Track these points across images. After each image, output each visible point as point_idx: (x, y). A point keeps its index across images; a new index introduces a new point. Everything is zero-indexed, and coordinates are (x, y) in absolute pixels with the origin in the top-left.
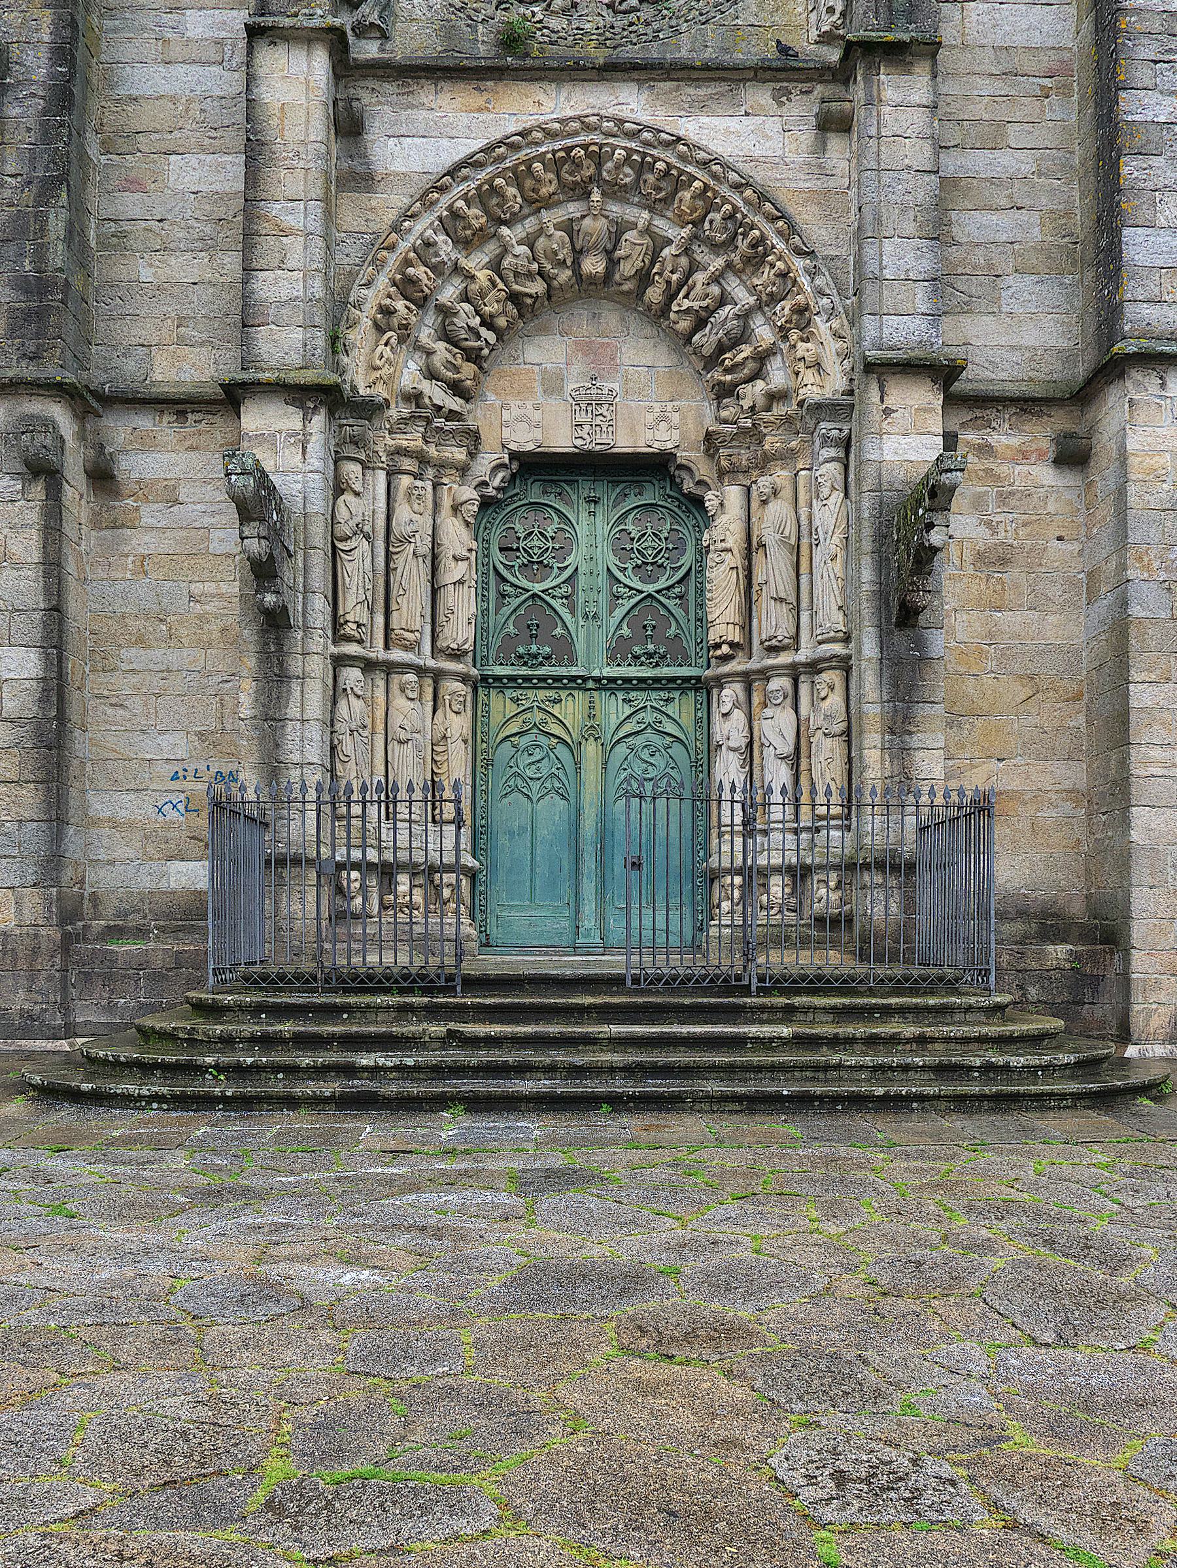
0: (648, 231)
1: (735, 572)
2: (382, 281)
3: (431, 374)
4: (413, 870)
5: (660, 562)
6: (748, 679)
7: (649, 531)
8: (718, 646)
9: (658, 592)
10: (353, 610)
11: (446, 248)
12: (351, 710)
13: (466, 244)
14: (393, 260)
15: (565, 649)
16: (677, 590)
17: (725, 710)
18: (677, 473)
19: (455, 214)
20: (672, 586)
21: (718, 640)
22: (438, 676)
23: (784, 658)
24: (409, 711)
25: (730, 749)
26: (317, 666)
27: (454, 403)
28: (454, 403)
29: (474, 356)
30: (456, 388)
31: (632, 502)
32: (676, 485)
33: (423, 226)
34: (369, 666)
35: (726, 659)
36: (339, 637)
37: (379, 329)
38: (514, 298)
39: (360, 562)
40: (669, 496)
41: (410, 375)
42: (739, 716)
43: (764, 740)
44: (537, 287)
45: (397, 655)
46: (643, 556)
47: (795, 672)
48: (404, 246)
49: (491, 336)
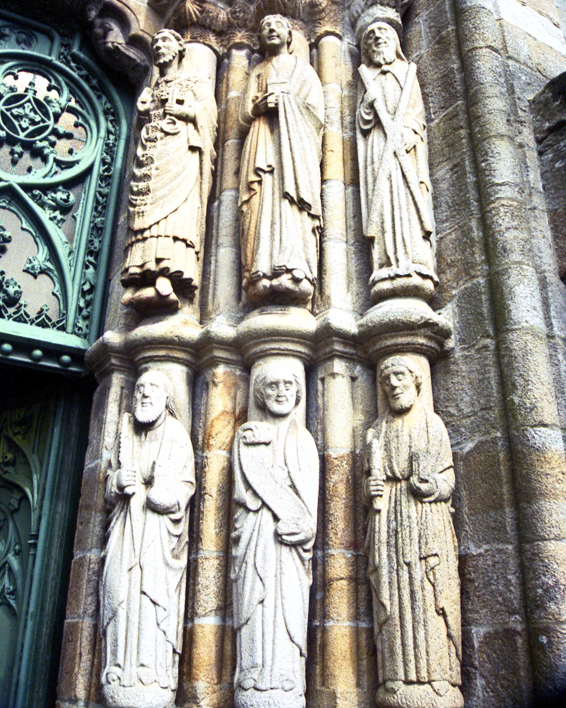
1: (197, 154)
5: (39, 144)
6: (198, 359)
7: (30, 95)
8: (147, 278)
9: (28, 188)
16: (60, 195)
17: (143, 416)
18: (98, 21)
20: (53, 187)
21: (152, 266)
23: (299, 319)
25: (151, 506)
32: (93, 42)
35: (161, 308)
40: (75, 58)
43: (240, 492)
46: (12, 127)
47: (318, 350)
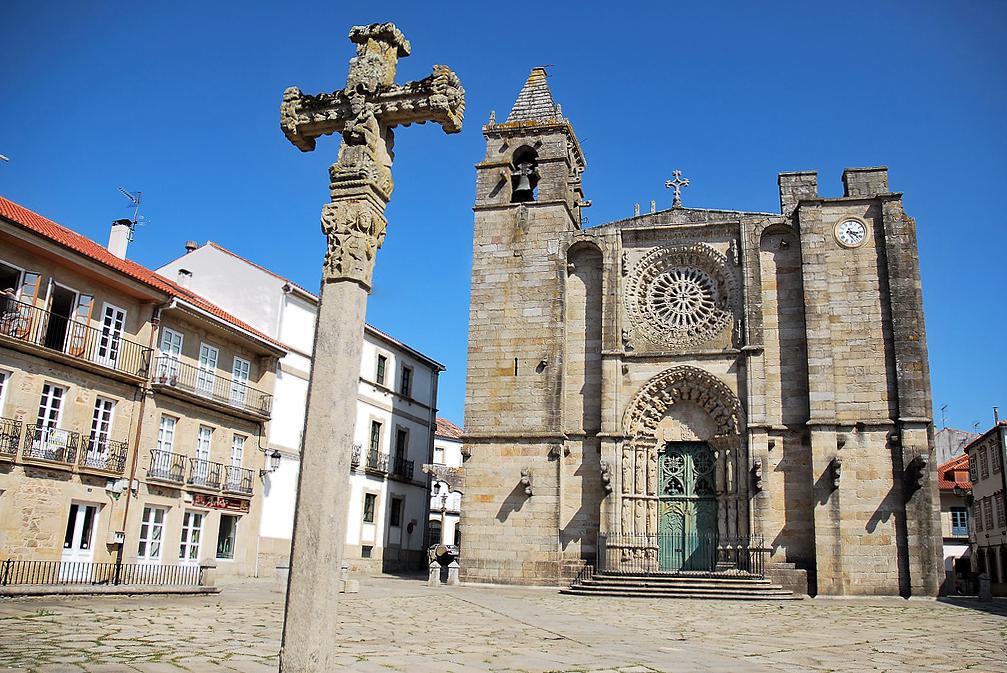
0: (698, 389)
2: (633, 407)
3: (645, 426)
4: (641, 549)
10: (629, 486)
11: (648, 397)
12: (627, 510)
13: (653, 396)
14: (636, 402)
15: (681, 490)
19: (651, 390)
22: (648, 500)
24: (642, 509)
26: (620, 501)
27: (651, 431)
28: (651, 431)
29: (656, 420)
30: (652, 428)
31: (698, 451)
33: (643, 393)
34: (631, 499)
36: (623, 493)
37: (633, 418)
38: (666, 405)
39: (629, 473)
41: (640, 426)
42: (724, 510)
44: (671, 402)
45: (638, 495)
48: (638, 398)
49: (660, 415)
